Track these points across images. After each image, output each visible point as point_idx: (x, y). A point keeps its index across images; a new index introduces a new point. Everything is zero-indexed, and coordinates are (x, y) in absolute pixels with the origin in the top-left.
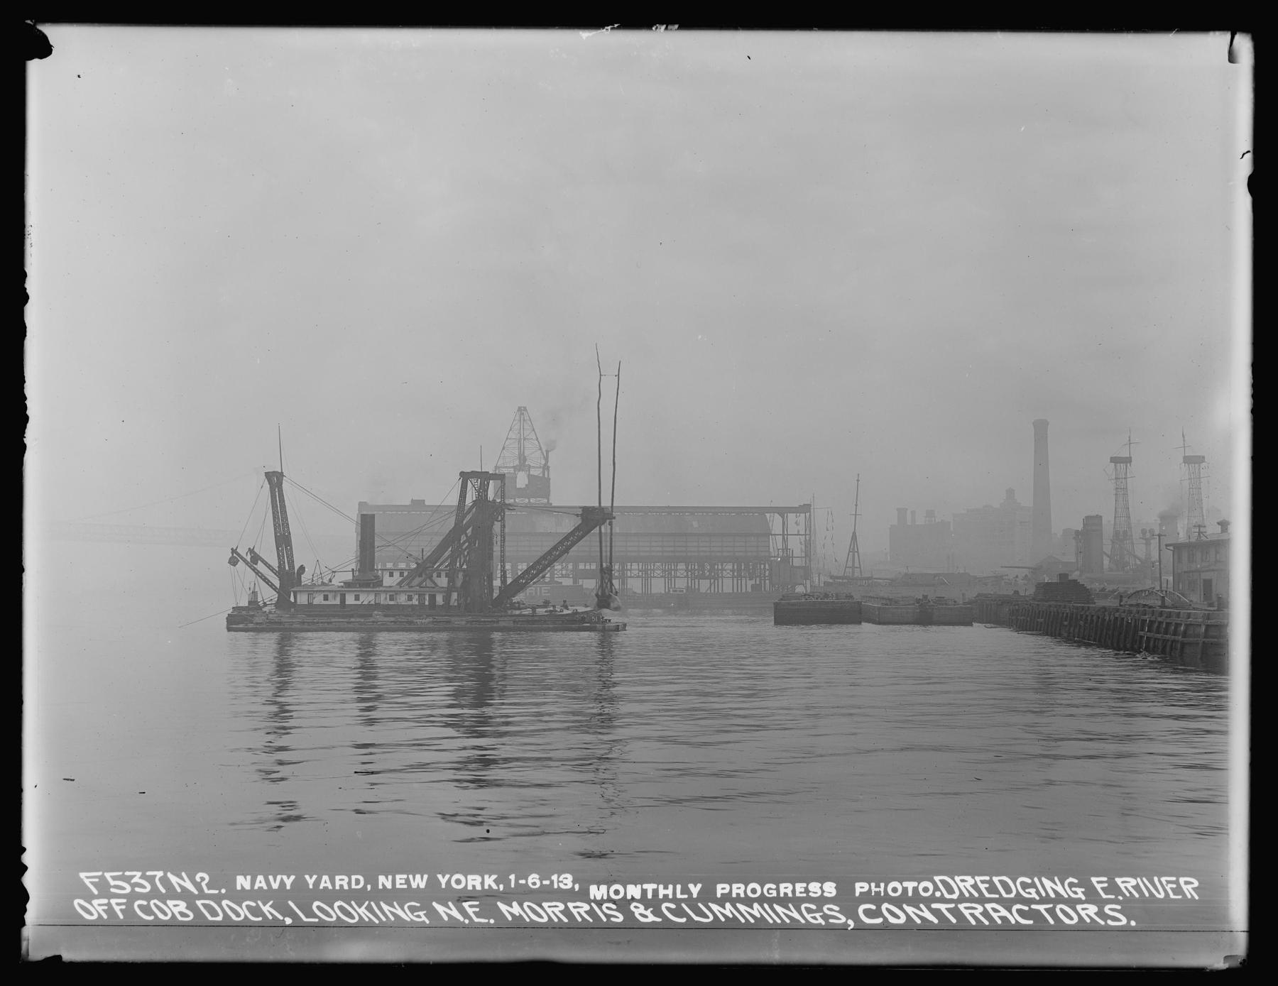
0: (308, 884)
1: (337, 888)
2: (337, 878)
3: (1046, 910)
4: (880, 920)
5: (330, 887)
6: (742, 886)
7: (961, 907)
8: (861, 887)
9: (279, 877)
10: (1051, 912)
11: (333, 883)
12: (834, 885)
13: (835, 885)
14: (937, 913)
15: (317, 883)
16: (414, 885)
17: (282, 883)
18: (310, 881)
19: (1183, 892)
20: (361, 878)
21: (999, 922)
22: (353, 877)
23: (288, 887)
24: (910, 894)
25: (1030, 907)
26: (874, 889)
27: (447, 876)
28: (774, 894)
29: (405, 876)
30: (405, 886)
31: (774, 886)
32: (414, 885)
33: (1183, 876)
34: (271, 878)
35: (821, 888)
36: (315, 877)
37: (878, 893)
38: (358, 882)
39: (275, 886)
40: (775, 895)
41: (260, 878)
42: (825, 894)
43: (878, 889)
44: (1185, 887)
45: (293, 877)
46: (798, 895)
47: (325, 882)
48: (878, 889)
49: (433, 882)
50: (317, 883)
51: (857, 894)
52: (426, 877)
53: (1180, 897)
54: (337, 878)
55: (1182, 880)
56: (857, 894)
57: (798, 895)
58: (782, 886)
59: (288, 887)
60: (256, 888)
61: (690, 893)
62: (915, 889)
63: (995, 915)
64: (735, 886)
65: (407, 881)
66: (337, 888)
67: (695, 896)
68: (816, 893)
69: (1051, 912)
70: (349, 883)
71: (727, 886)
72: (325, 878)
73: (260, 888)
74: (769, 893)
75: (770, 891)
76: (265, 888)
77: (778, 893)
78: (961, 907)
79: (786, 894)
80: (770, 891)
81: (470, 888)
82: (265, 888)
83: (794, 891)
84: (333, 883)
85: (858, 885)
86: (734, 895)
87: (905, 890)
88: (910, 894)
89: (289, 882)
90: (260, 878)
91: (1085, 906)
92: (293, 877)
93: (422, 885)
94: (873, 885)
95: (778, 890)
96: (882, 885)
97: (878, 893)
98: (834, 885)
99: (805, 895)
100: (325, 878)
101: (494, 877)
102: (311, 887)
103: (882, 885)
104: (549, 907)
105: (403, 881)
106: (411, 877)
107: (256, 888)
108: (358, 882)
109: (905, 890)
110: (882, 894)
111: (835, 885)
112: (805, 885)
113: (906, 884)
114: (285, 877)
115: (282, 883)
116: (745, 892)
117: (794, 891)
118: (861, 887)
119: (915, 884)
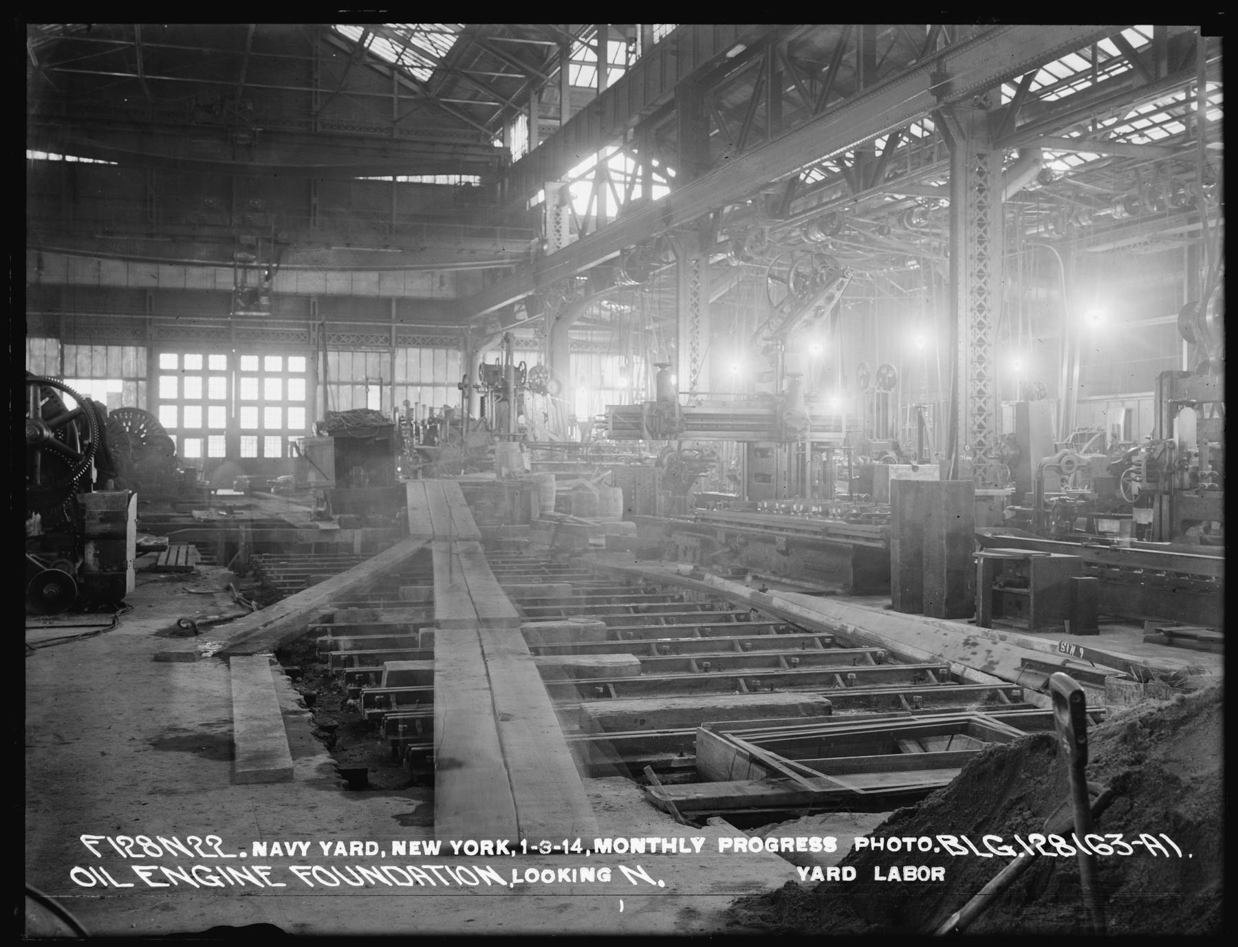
0: (322, 850)
1: (352, 854)
2: (353, 844)
5: (345, 854)
9: (295, 844)
11: (348, 850)
15: (332, 849)
16: (427, 852)
17: (298, 850)
18: (326, 847)
20: (375, 844)
22: (368, 844)
23: (304, 854)
24: (909, 849)
26: (874, 845)
29: (419, 843)
31: (776, 841)
32: (427, 852)
34: (287, 844)
35: (824, 846)
36: (330, 844)
37: (877, 848)
38: (372, 848)
39: (291, 853)
41: (276, 845)
43: (878, 845)
45: (308, 844)
47: (340, 849)
48: (878, 845)
50: (332, 849)
52: (439, 843)
54: (353, 844)
57: (799, 849)
58: (783, 840)
59: (304, 854)
60: (272, 854)
62: (914, 845)
65: (421, 848)
66: (352, 854)
67: (698, 851)
70: (364, 850)
71: (729, 840)
72: (340, 844)
73: (277, 855)
76: (281, 854)
77: (780, 848)
79: (787, 849)
82: (281, 854)
83: (795, 847)
84: (348, 850)
86: (736, 850)
87: (904, 845)
88: (909, 849)
89: (304, 847)
90: (276, 845)
92: (308, 844)
93: (436, 852)
94: (873, 839)
95: (779, 844)
96: (882, 840)
99: (806, 850)
100: (340, 844)
102: (326, 853)
103: (882, 840)
105: (417, 848)
106: (424, 843)
107: (272, 854)
108: (372, 848)
112: (806, 839)
113: (905, 840)
114: (300, 844)
115: (298, 850)
116: (747, 846)
119: (914, 840)
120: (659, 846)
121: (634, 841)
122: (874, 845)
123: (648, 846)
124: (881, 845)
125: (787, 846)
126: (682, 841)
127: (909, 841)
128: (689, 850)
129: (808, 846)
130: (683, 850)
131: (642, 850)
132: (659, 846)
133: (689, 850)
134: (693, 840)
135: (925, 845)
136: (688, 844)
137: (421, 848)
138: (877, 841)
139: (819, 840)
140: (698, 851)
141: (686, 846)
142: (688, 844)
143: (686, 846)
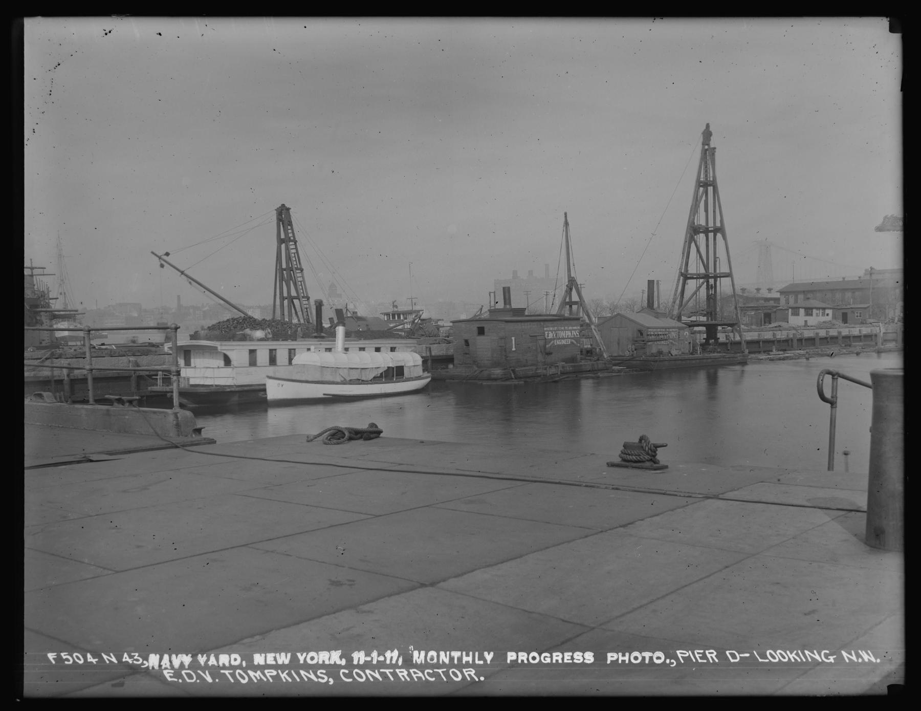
3: (229, 673)
4: (350, 680)
6: (526, 655)
7: (397, 671)
8: (612, 657)
10: (233, 675)
11: (217, 660)
12: (592, 654)
13: (593, 654)
14: (383, 675)
16: (280, 662)
19: (708, 658)
21: (416, 680)
24: (647, 661)
25: (433, 671)
26: (621, 658)
27: (305, 654)
28: (548, 660)
30: (274, 663)
31: (548, 655)
33: (678, 650)
35: (583, 656)
37: (623, 661)
40: (550, 662)
42: (586, 661)
43: (624, 658)
44: (709, 656)
46: (566, 661)
47: (212, 661)
49: (294, 659)
51: (609, 662)
53: (705, 661)
55: (707, 652)
56: (609, 662)
57: (566, 661)
58: (554, 654)
61: (485, 660)
62: (651, 658)
63: (414, 676)
64: (520, 654)
65: (275, 659)
67: (489, 662)
68: (579, 660)
69: (233, 675)
71: (514, 654)
74: (544, 660)
75: (546, 659)
77: (552, 660)
78: (397, 671)
80: (546, 659)
81: (321, 662)
83: (563, 659)
85: (609, 655)
87: (644, 658)
88: (647, 661)
90: (166, 657)
91: (402, 670)
93: (287, 662)
94: (620, 654)
95: (551, 657)
97: (623, 661)
98: (592, 654)
99: (571, 661)
101: (339, 653)
103: (627, 654)
104: (268, 672)
106: (278, 655)
108: (235, 660)
109: (644, 658)
110: (627, 662)
111: (593, 654)
112: (570, 654)
113: (644, 654)
116: (528, 659)
117: (563, 659)
118: (612, 657)
119: (650, 654)
120: (460, 659)
121: (442, 654)
122: (621, 658)
123: (452, 659)
124: (626, 658)
125: (557, 658)
126: (477, 654)
127: (647, 655)
128: (481, 662)
129: (572, 658)
130: (477, 662)
131: (447, 661)
132: (460, 659)
133: (481, 662)
134: (486, 653)
135: (658, 658)
136: (482, 657)
137: (275, 659)
138: (624, 655)
139: (581, 654)
140: (489, 662)
141: (479, 660)
142: (482, 657)
143: (479, 660)
